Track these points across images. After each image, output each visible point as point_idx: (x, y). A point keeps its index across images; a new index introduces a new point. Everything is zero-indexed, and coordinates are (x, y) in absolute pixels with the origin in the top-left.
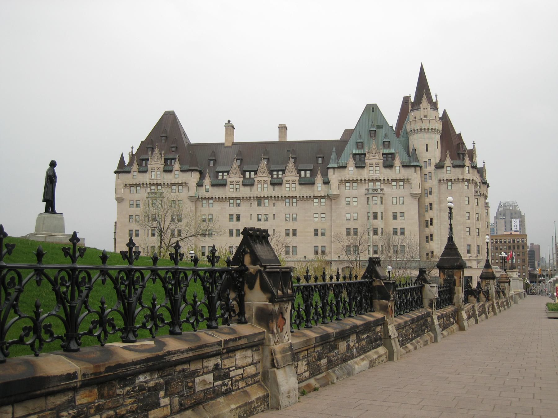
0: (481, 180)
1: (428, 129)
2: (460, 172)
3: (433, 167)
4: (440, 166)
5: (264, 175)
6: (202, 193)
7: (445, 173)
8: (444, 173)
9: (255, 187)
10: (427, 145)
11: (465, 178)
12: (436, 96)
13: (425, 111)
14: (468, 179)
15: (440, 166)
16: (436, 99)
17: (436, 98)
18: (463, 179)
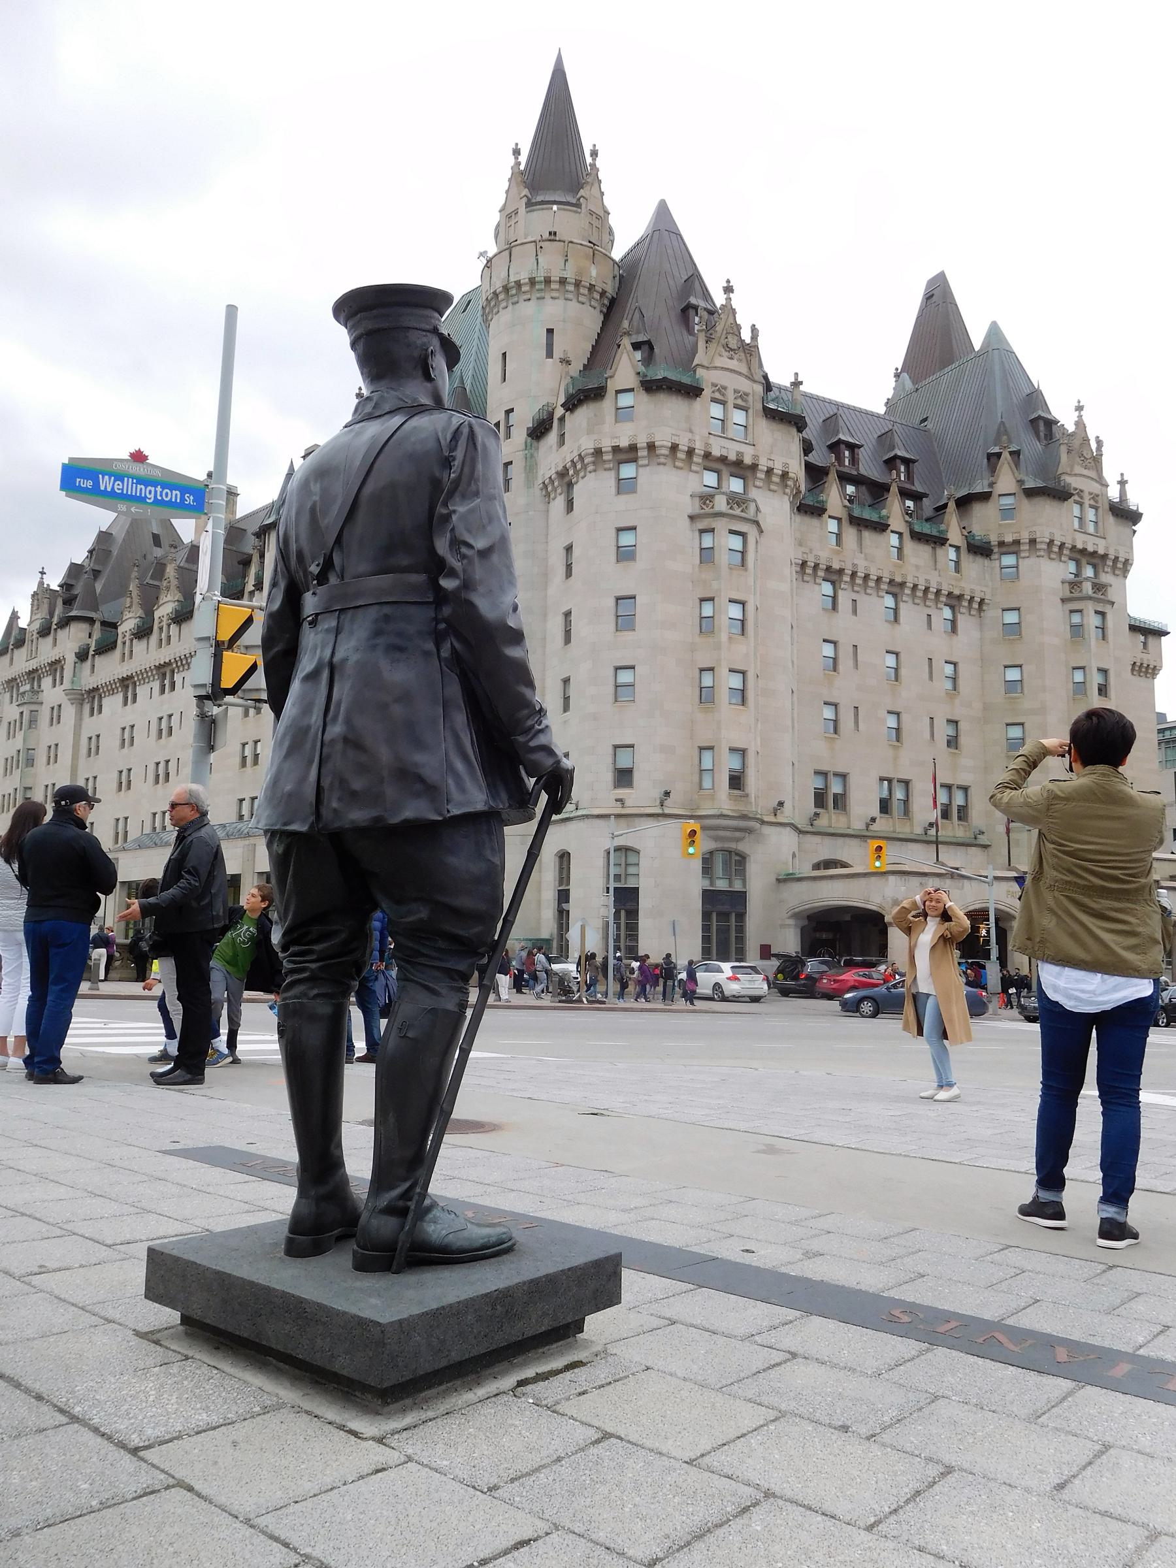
0: (1021, 482)
1: (506, 289)
2: (584, 424)
3: (520, 435)
4: (539, 430)
5: (169, 598)
6: (88, 680)
7: (555, 447)
8: (551, 447)
9: (154, 638)
10: (505, 354)
11: (607, 444)
12: (594, 154)
13: (512, 223)
14: (624, 443)
15: (539, 430)
16: (593, 165)
17: (594, 160)
18: (598, 452)
